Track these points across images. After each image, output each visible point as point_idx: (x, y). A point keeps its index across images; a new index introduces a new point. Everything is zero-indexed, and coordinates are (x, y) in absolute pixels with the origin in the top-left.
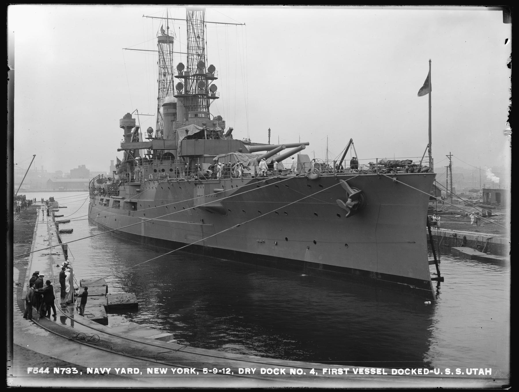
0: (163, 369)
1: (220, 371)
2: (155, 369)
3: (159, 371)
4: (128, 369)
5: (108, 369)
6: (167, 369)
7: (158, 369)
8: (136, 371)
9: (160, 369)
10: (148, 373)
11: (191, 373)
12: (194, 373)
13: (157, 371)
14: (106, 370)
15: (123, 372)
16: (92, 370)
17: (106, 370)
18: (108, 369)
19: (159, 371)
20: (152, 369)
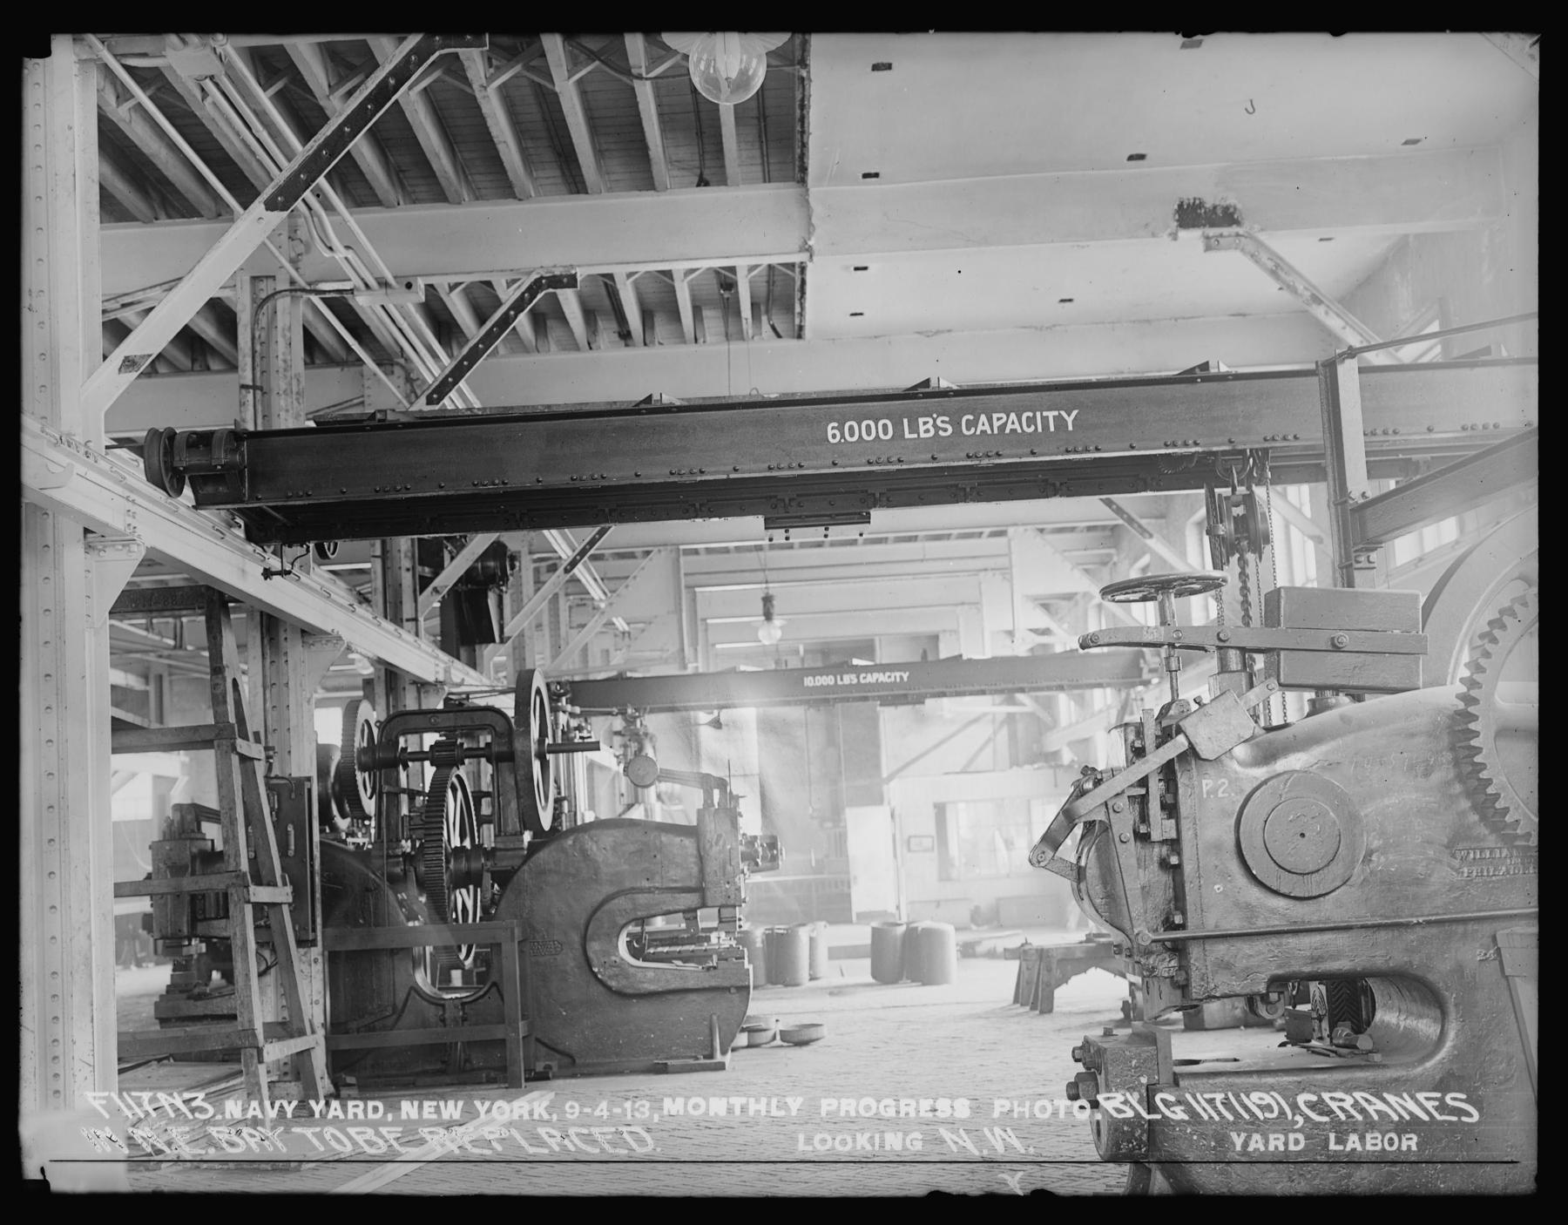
0: (451, 1103)
1: (617, 1110)
2: (426, 1104)
3: (438, 1110)
4: (351, 1103)
5: (290, 1103)
6: (460, 1103)
7: (435, 1103)
8: (376, 1109)
9: (442, 1104)
10: (404, 1116)
11: (536, 1117)
12: (546, 1117)
13: (432, 1110)
14: (281, 1107)
15: (336, 1114)
16: (240, 1108)
17: (281, 1107)
18: (290, 1103)
19: (437, 1107)
20: (416, 1103)
